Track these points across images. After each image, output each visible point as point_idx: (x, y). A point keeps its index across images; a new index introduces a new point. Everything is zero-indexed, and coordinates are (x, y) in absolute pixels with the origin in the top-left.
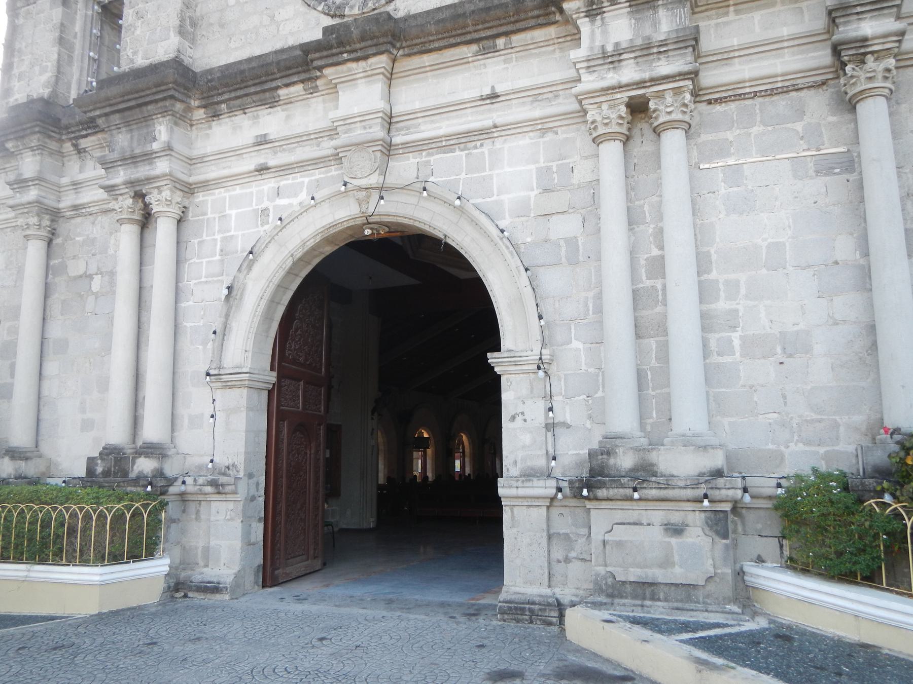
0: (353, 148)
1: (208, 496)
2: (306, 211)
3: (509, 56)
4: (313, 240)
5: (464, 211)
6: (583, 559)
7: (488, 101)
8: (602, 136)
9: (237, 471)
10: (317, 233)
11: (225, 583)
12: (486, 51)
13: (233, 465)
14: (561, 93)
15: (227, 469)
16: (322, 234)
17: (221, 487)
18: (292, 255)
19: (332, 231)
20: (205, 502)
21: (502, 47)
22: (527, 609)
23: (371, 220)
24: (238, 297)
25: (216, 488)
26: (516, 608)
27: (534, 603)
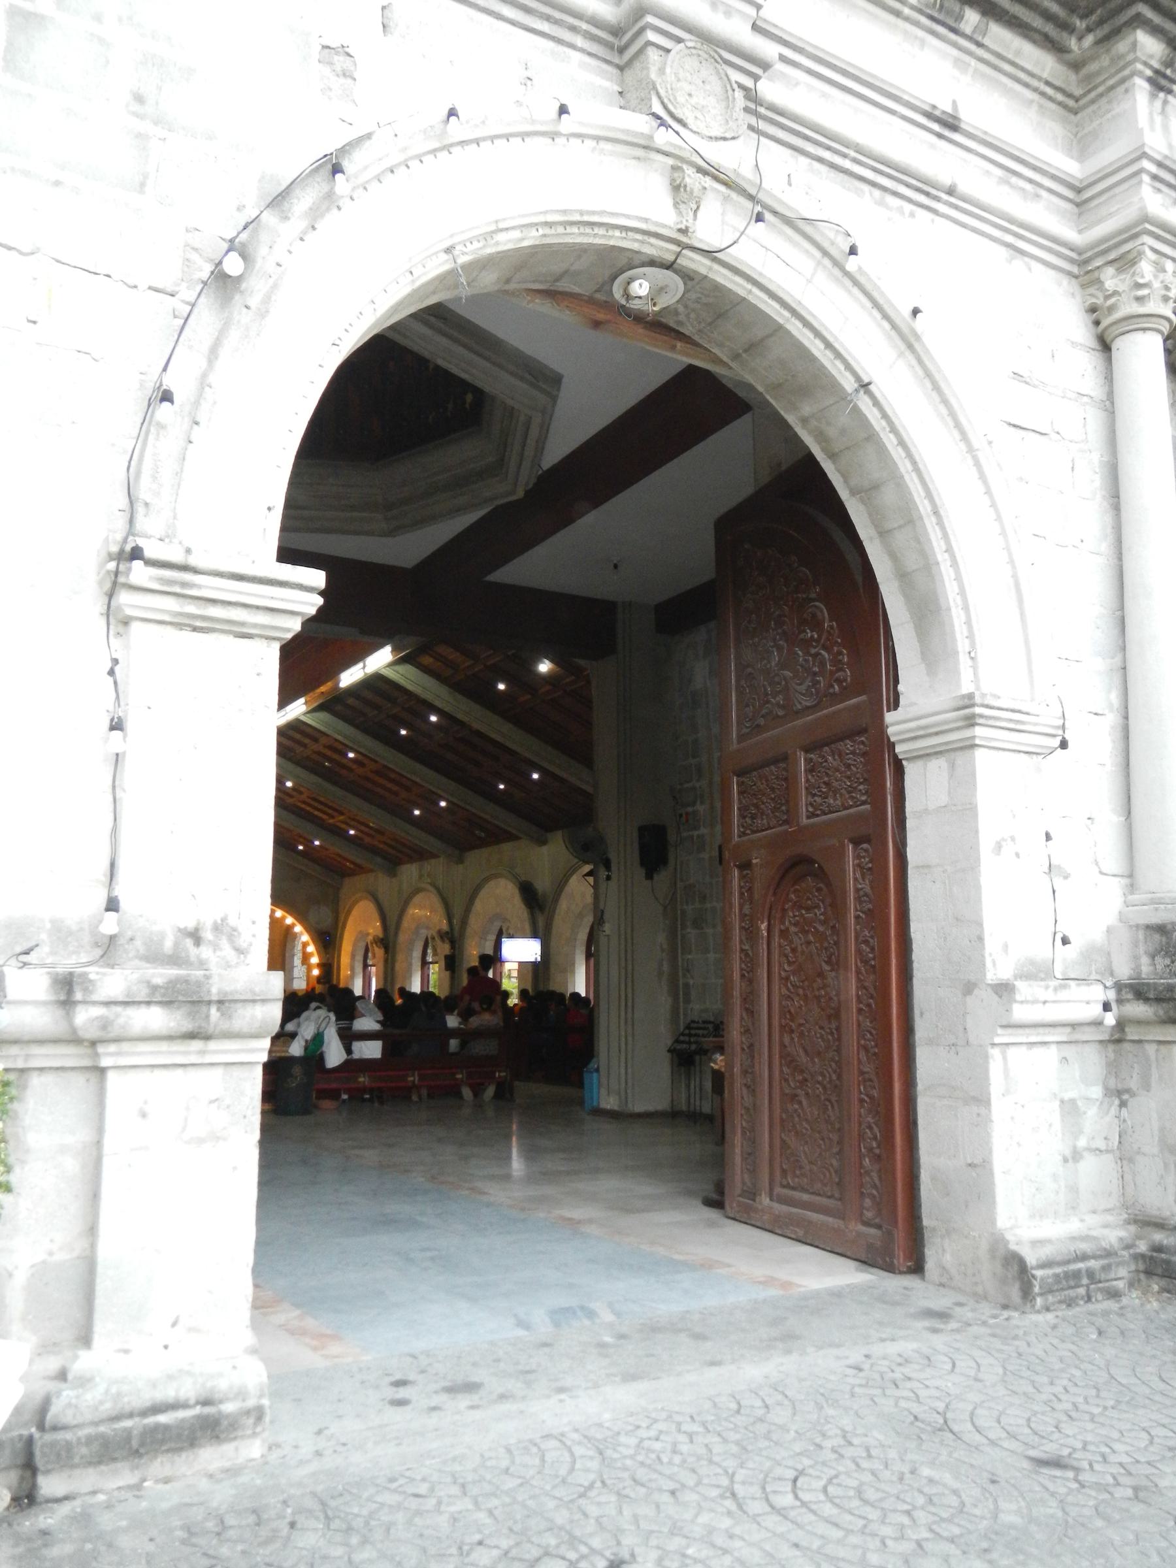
0: (691, 40)
1: (112, 1048)
2: (523, 135)
3: (967, 58)
4: (516, 234)
5: (917, 346)
6: (1097, 1149)
7: (936, 127)
8: (1154, 319)
9: (240, 951)
10: (542, 219)
11: (241, 1394)
12: (941, 17)
13: (217, 928)
14: (1044, 194)
15: (189, 942)
16: (547, 231)
17: (213, 1011)
18: (449, 250)
19: (576, 237)
20: (48, 1078)
21: (968, 30)
22: (1084, 1272)
23: (694, 262)
24: (254, 302)
25: (192, 1015)
26: (1067, 1275)
27: (1084, 1257)
